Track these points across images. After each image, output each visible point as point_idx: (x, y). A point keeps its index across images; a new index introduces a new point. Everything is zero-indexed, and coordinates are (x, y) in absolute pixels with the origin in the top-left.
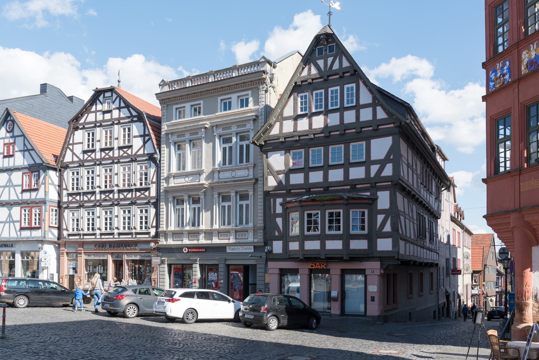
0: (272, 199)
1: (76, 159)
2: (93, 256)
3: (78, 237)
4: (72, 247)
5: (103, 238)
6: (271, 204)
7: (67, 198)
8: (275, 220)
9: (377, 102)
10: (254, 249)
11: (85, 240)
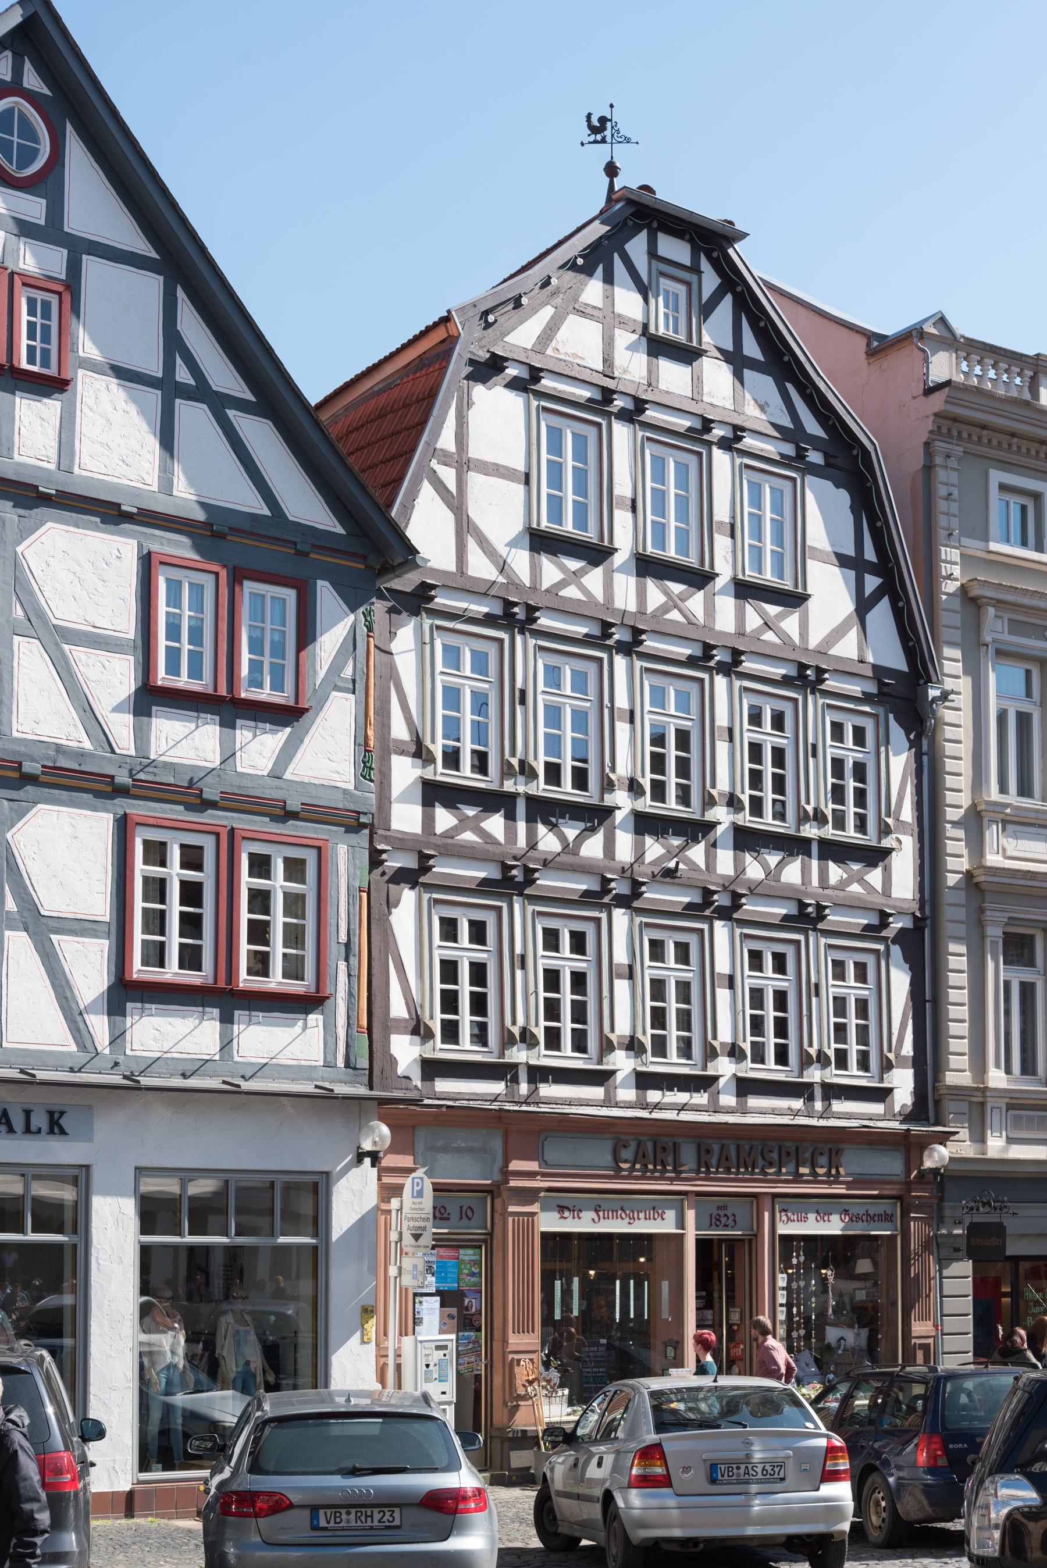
1: (481, 567)
2: (588, 1215)
3: (498, 1087)
4: (458, 1150)
5: (657, 1106)
7: (417, 810)
11: (544, 1108)
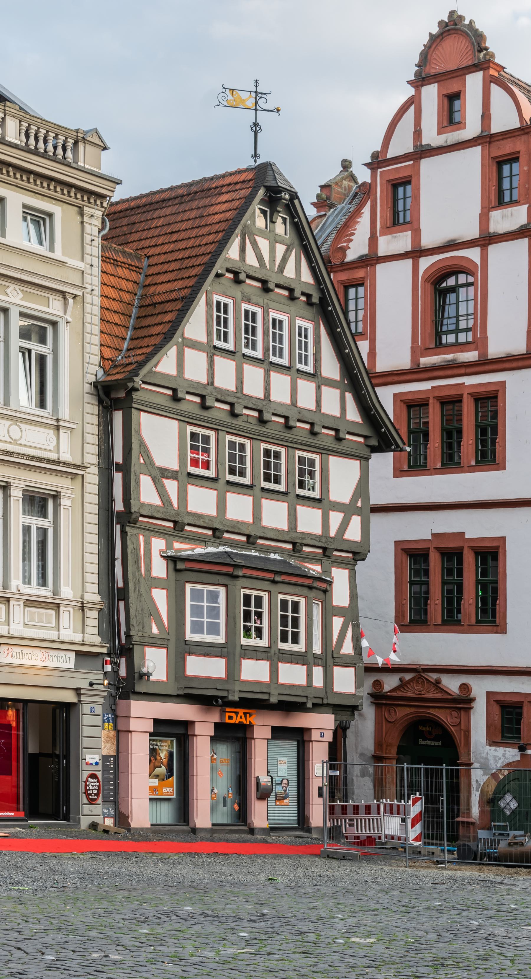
0: (141, 537)
6: (140, 552)
8: (151, 592)
9: (346, 382)
10: (76, 659)
